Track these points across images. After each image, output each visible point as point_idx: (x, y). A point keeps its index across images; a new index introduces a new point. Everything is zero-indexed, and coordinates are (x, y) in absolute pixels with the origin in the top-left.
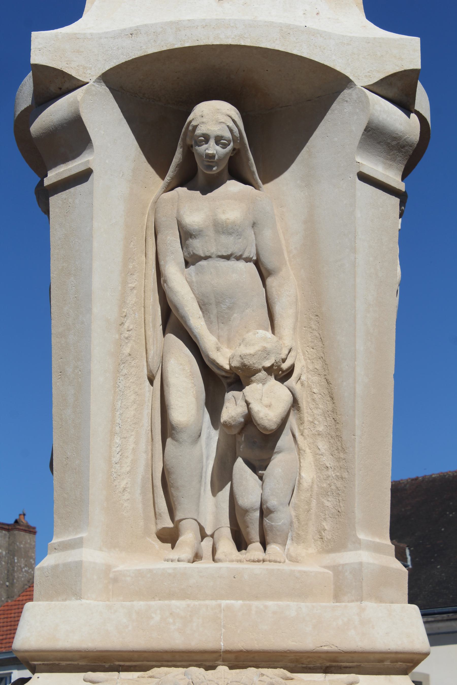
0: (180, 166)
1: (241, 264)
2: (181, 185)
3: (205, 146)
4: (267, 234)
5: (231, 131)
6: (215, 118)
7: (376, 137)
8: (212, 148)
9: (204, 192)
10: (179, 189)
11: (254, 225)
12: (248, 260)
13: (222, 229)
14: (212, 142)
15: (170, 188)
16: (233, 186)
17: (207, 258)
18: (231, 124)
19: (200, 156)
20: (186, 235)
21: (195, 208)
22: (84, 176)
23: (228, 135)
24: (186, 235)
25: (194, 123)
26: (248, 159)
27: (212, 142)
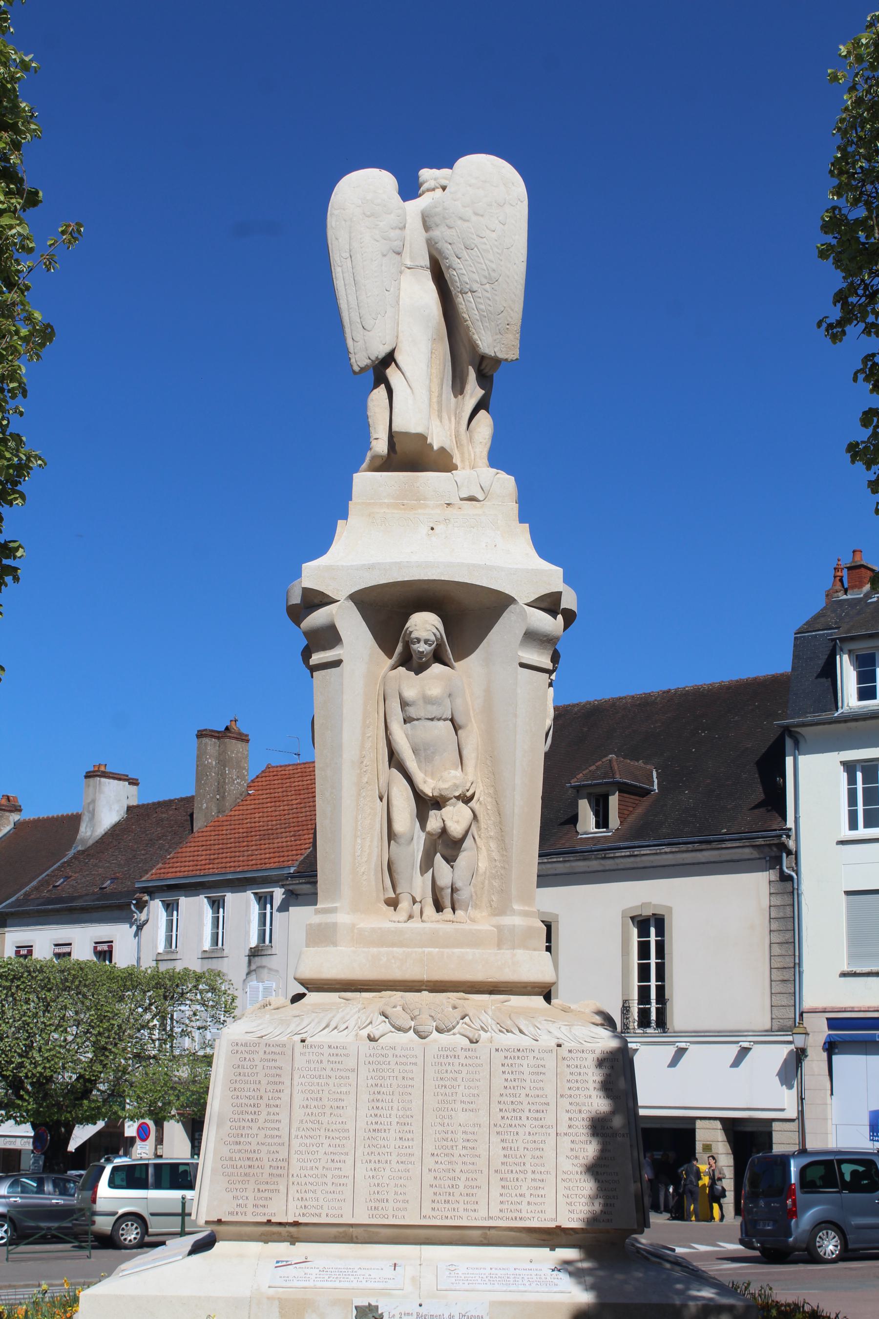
0: (401, 654)
1: (441, 723)
2: (402, 665)
3: (418, 645)
4: (459, 701)
5: (435, 635)
6: (425, 625)
7: (532, 637)
8: (422, 647)
9: (417, 674)
10: (400, 668)
11: (450, 695)
12: (445, 720)
13: (428, 701)
14: (422, 643)
15: (394, 667)
16: (437, 668)
17: (418, 719)
18: (435, 631)
19: (415, 651)
20: (404, 704)
21: (411, 685)
22: (337, 663)
23: (433, 638)
24: (404, 704)
25: (410, 629)
26: (447, 651)
27: (422, 643)
